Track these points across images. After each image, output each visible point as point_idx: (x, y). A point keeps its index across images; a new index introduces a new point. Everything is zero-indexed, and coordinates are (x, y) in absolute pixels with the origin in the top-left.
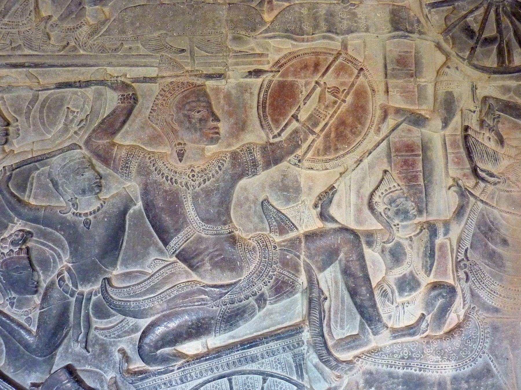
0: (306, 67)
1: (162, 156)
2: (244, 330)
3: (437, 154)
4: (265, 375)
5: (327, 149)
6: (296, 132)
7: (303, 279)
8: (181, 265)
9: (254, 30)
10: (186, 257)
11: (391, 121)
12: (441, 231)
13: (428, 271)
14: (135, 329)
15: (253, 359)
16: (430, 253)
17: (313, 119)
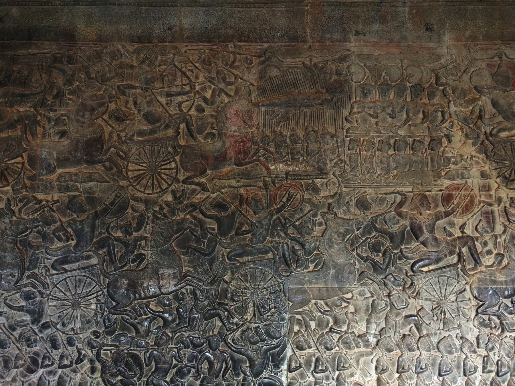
0: (455, 189)
1: (415, 214)
2: (441, 264)
3: (496, 214)
4: (448, 277)
5: (463, 213)
6: (453, 208)
7: (457, 250)
8: (422, 245)
9: (440, 178)
10: (424, 243)
11: (482, 205)
12: (499, 237)
13: (495, 249)
14: (410, 263)
15: (445, 272)
16: (496, 244)
17: (458, 204)
